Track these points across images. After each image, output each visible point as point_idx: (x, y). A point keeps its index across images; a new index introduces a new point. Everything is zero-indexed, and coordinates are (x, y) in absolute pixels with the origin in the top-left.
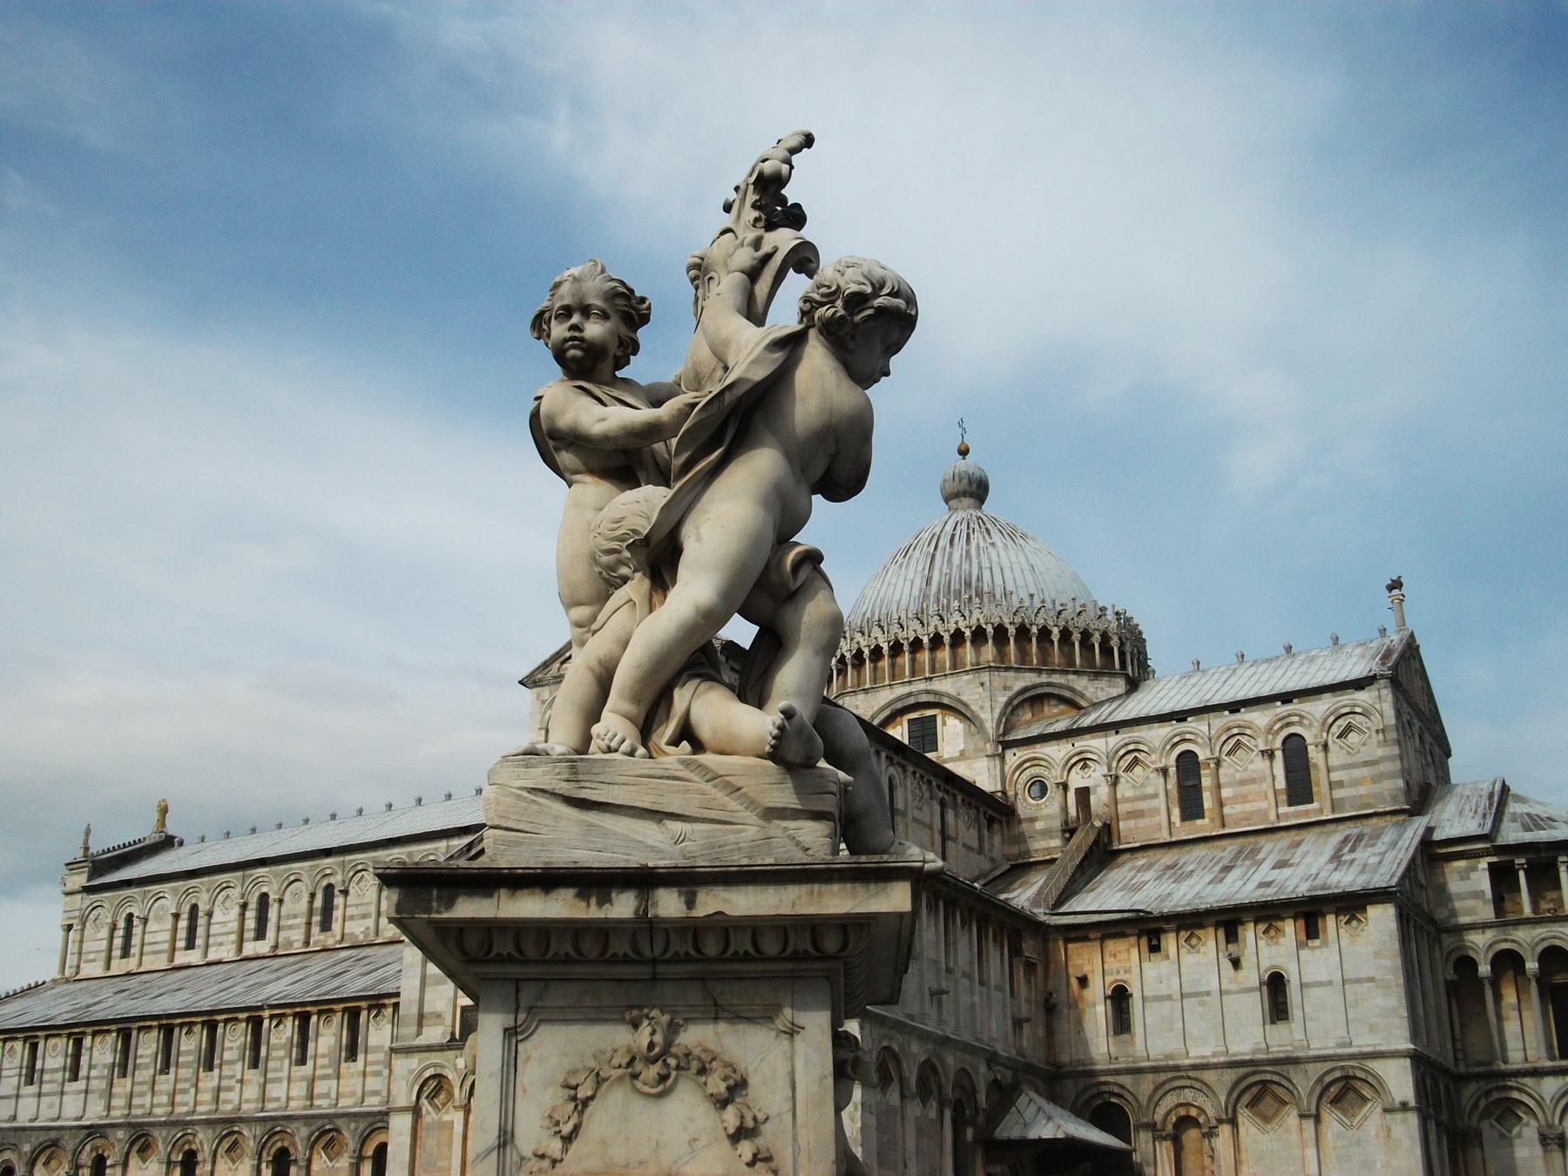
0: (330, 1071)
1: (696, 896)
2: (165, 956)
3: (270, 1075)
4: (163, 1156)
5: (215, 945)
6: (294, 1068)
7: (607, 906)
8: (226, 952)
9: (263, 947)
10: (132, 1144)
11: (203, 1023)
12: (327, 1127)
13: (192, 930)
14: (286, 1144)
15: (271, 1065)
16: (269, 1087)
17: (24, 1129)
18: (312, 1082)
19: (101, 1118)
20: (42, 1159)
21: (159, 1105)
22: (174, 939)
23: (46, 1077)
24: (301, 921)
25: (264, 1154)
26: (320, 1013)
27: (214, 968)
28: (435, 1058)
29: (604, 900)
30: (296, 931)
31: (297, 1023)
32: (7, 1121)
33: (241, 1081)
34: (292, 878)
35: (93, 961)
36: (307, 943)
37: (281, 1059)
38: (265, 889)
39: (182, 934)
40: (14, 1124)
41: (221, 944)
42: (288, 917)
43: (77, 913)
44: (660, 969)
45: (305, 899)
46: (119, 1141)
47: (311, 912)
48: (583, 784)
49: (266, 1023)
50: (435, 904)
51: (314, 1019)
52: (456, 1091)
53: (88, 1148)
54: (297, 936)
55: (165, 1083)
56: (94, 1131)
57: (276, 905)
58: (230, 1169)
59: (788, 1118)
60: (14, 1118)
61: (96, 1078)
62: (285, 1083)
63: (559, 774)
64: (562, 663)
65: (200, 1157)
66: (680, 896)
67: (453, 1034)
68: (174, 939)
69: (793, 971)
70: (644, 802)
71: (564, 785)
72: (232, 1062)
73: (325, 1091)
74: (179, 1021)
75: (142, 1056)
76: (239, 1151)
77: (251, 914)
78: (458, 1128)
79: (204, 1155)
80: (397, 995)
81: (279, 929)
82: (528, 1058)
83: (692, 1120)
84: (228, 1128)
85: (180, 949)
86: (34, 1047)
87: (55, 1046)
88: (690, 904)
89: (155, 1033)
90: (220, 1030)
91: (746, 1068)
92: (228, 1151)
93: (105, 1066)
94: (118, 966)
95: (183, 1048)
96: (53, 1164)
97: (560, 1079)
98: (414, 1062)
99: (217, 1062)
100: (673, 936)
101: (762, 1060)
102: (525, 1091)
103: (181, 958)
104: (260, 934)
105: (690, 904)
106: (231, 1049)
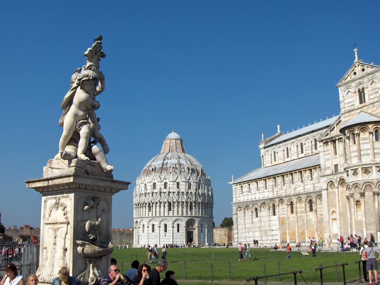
0: (318, 181)
2: (283, 160)
3: (305, 184)
4: (286, 203)
5: (293, 156)
6: (310, 182)
8: (296, 157)
9: (303, 155)
10: (279, 201)
11: (290, 174)
12: (319, 194)
13: (288, 153)
14: (311, 199)
15: (305, 181)
16: (305, 186)
17: (258, 200)
18: (314, 184)
19: (272, 197)
20: (262, 206)
21: (292, 191)
22: (284, 156)
23: (260, 189)
24: (310, 148)
25: (307, 201)
26: (314, 169)
27: (293, 161)
28: (330, 177)
30: (309, 151)
31: (309, 171)
32: (254, 199)
33: (299, 186)
34: (307, 138)
35: (269, 163)
36: (312, 153)
37: (307, 180)
38: (301, 142)
39: (286, 154)
40: (256, 199)
41: (294, 155)
42: (307, 147)
43: (263, 153)
45: (310, 143)
46: (277, 201)
47: (312, 146)
49: (303, 172)
51: (313, 170)
52: (335, 184)
53: (271, 203)
54: (310, 151)
55: (284, 188)
56: (271, 199)
57: (304, 145)
58: (300, 205)
60: (255, 198)
61: (270, 188)
62: (309, 185)
64: (345, 80)
65: (293, 203)
67: (333, 171)
68: (284, 156)
72: (297, 182)
73: (317, 186)
74: (285, 174)
75: (278, 183)
76: (301, 201)
77: (299, 148)
78: (337, 193)
79: (294, 202)
80: (320, 165)
81: (306, 150)
84: (298, 196)
85: (286, 158)
86: (257, 182)
87: (261, 183)
89: (280, 177)
90: (293, 175)
92: (299, 201)
93: (272, 185)
94: (274, 163)
95: (286, 180)
96: (265, 207)
98: (325, 178)
99: (294, 182)
103: (286, 160)
104: (302, 152)
106: (296, 179)
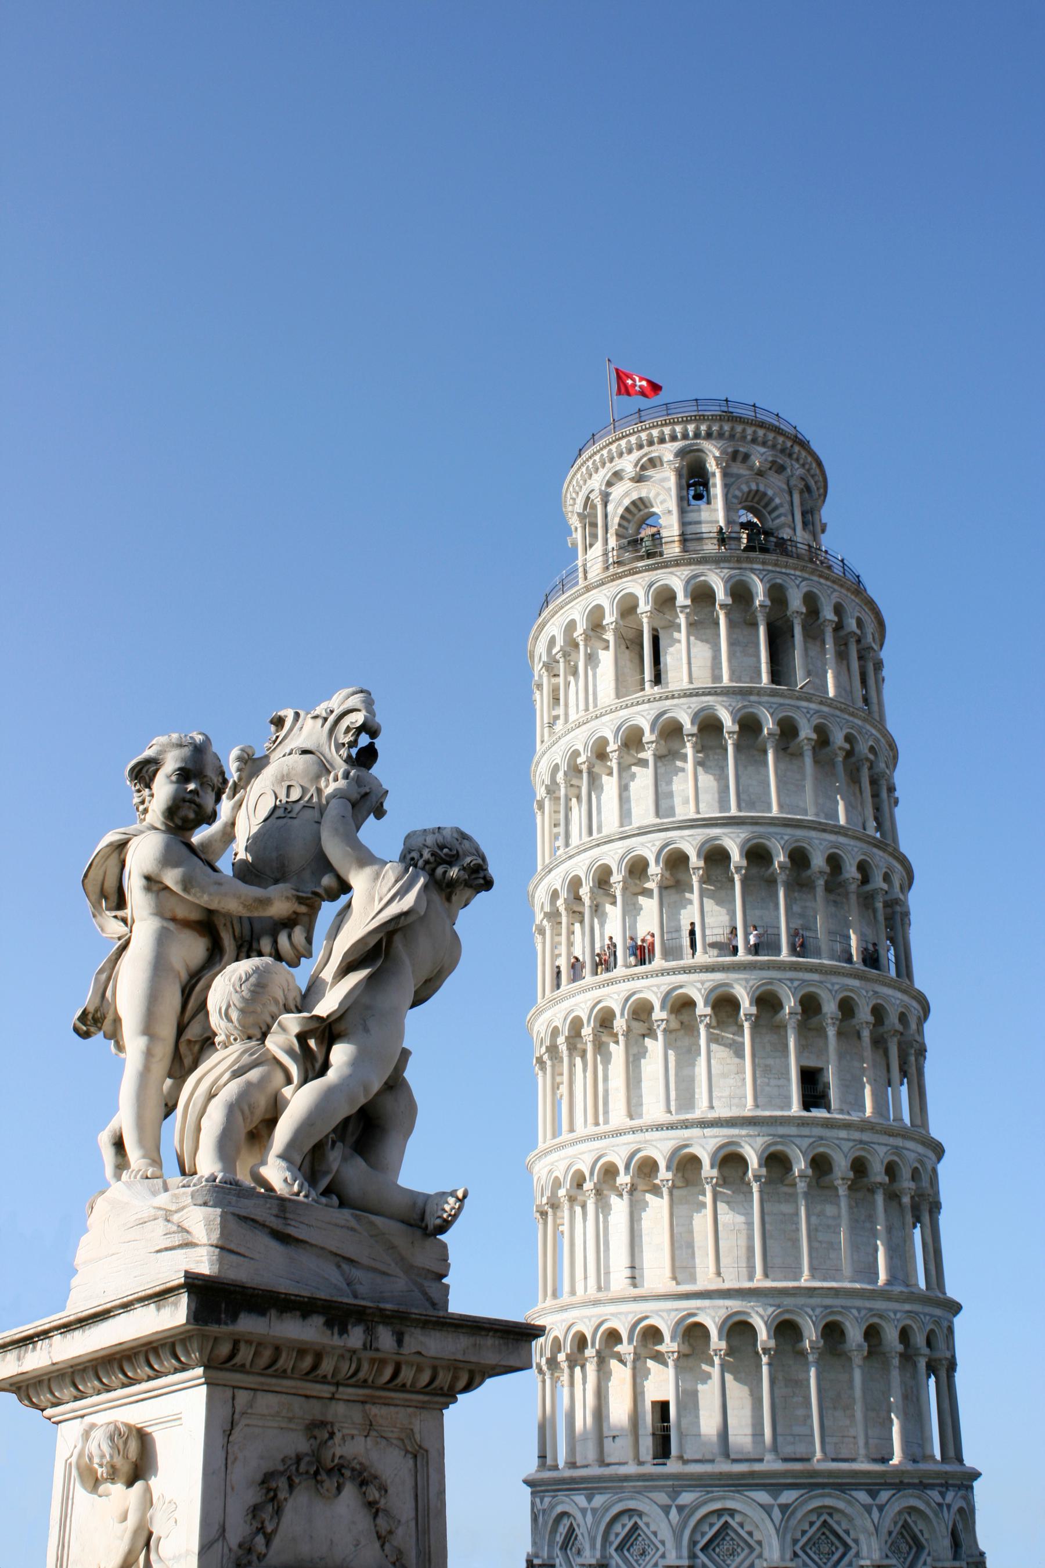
1: (403, 1337)
7: (345, 1336)
29: (343, 1331)
44: (341, 1389)
48: (289, 1222)
50: (223, 1316)
59: (413, 1524)
63: (270, 1208)
66: (393, 1335)
69: (424, 1402)
70: (332, 1245)
71: (273, 1219)
82: (236, 1459)
83: (354, 1523)
88: (400, 1342)
91: (386, 1482)
97: (259, 1477)
100: (365, 1366)
101: (396, 1475)
102: (233, 1489)
105: (400, 1342)
